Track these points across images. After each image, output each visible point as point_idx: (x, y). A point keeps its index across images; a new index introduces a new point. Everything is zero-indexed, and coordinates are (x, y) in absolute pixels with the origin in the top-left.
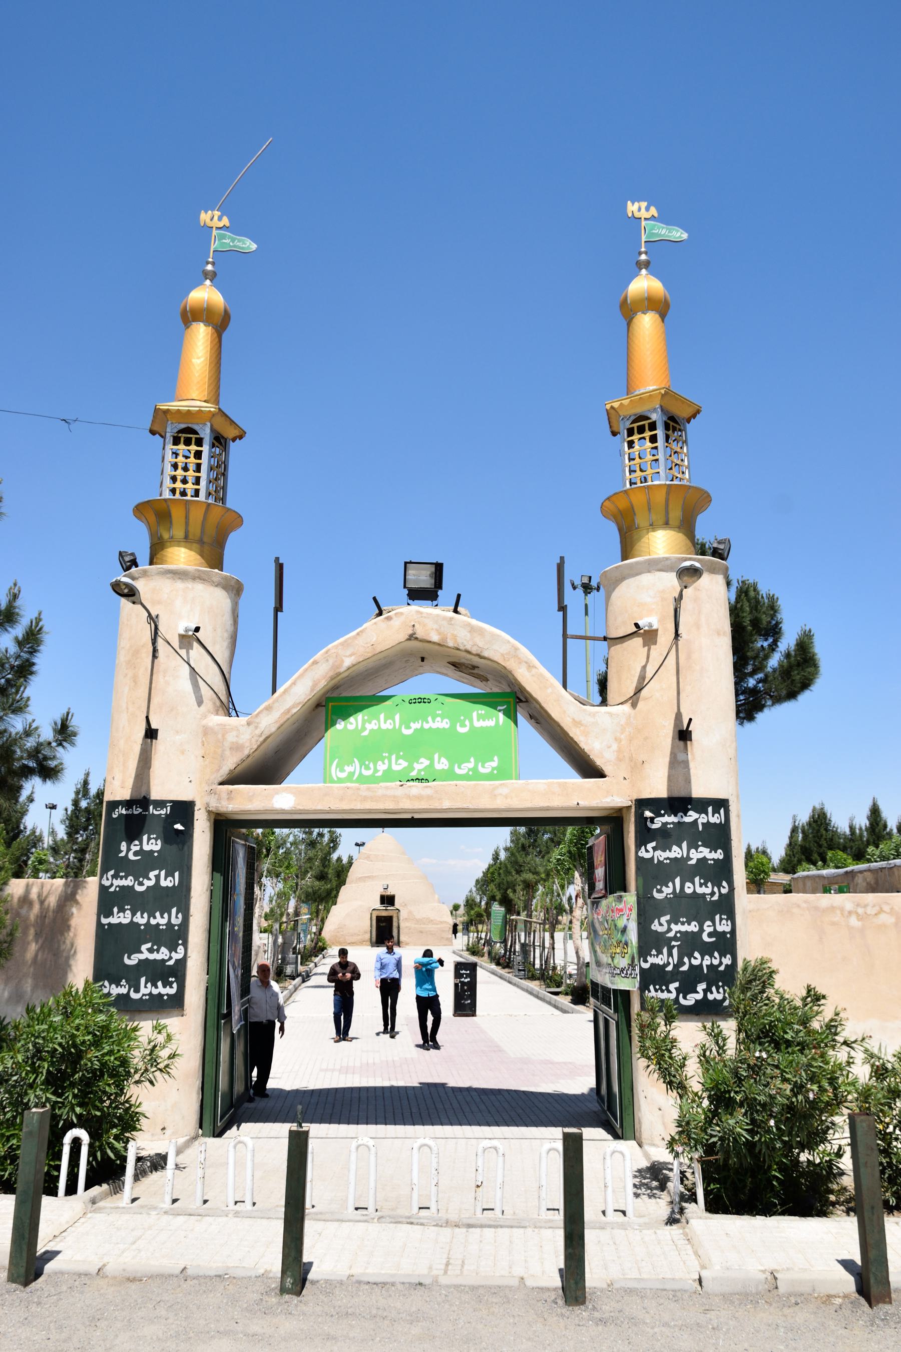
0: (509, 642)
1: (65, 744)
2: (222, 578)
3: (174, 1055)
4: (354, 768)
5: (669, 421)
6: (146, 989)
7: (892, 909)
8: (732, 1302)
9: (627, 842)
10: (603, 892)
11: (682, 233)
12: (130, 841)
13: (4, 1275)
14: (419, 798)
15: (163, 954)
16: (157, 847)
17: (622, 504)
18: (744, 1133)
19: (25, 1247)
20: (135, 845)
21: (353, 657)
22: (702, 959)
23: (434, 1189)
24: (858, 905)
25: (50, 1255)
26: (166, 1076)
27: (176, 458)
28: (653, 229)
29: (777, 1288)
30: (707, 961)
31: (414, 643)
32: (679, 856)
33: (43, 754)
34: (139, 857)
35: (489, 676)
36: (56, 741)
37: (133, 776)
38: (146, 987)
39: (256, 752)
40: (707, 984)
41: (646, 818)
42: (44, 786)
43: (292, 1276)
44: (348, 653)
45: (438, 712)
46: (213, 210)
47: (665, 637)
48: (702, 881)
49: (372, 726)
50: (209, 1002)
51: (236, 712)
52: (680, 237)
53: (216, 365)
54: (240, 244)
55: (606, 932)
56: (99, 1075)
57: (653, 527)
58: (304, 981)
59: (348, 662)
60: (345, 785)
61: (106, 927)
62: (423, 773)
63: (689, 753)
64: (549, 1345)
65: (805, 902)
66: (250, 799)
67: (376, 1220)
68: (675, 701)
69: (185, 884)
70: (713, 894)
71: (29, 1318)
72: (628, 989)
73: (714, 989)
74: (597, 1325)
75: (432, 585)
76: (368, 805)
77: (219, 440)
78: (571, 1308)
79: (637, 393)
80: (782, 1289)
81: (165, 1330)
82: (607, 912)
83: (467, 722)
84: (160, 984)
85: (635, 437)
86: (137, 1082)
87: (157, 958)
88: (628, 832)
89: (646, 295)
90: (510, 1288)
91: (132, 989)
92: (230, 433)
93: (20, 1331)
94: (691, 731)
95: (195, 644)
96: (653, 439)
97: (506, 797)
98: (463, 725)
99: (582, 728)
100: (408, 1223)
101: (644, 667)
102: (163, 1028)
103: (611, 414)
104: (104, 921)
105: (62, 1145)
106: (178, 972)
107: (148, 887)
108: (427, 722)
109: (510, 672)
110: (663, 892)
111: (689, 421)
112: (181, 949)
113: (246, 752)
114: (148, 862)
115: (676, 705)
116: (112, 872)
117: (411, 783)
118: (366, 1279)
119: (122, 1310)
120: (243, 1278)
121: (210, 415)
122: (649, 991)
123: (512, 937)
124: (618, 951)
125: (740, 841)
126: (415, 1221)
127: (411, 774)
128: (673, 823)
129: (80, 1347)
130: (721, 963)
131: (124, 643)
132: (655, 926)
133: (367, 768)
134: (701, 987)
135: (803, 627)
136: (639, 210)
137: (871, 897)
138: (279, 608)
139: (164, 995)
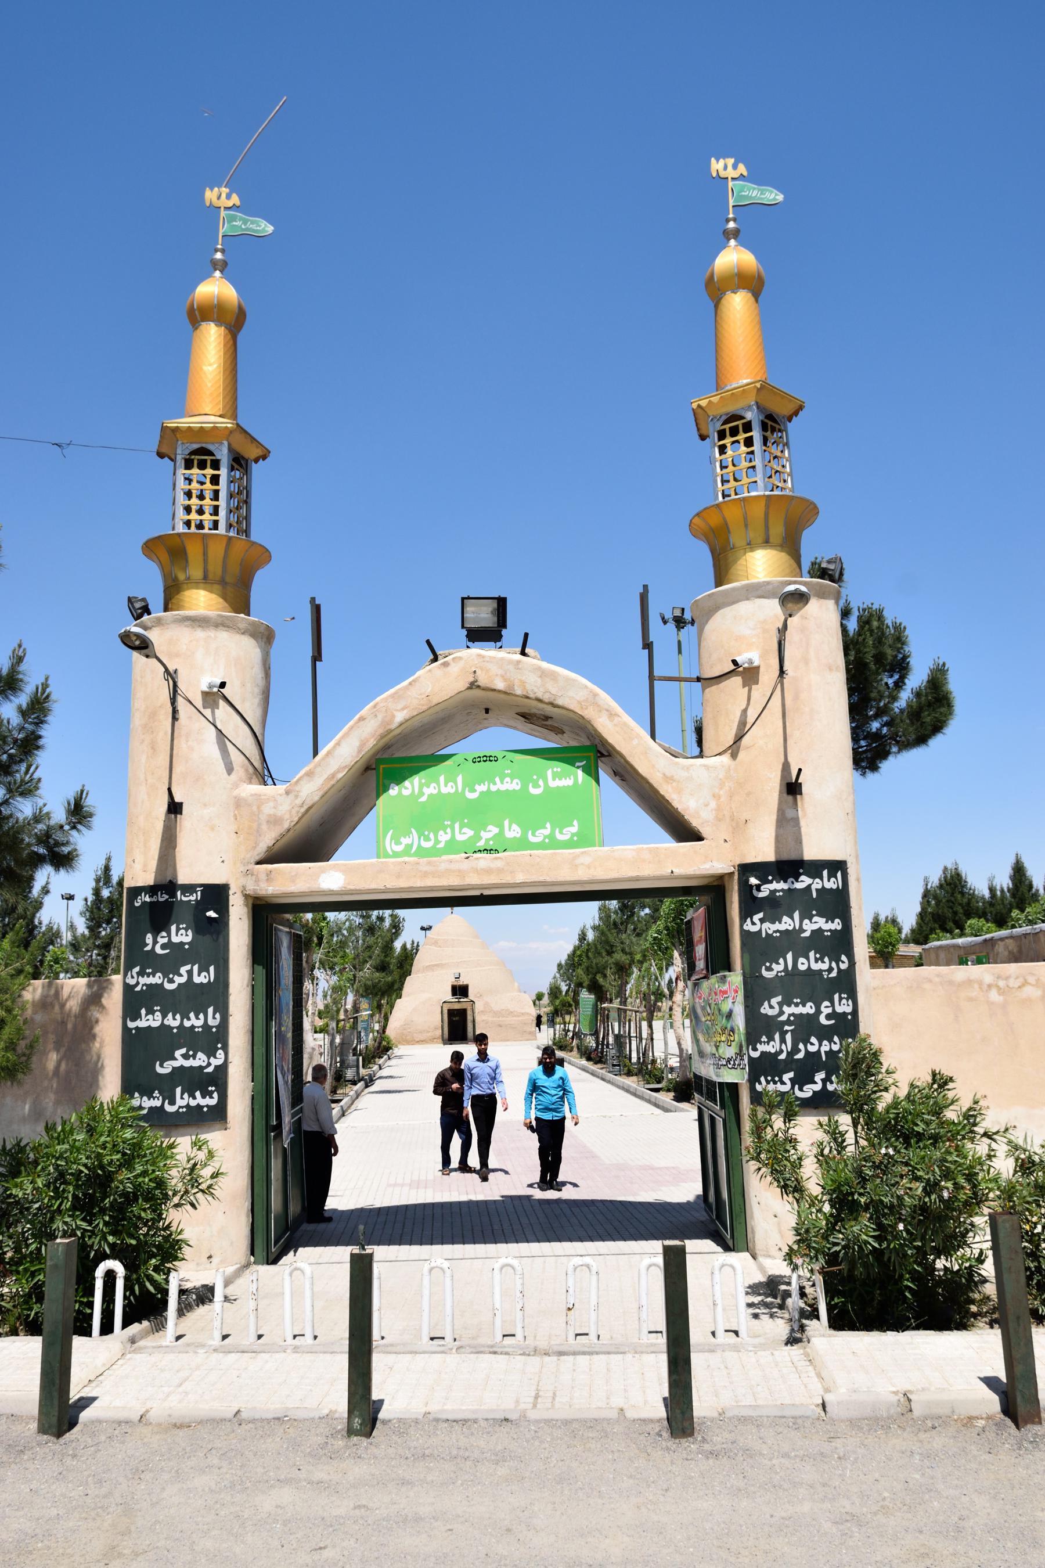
0: (586, 687)
2: (249, 624)
3: (217, 1174)
4: (412, 839)
5: (766, 421)
6: (182, 1100)
7: (1038, 980)
8: (860, 1428)
9: (731, 915)
10: (704, 972)
11: (776, 195)
12: (156, 933)
13: (34, 1426)
14: (488, 871)
15: (200, 1060)
16: (188, 939)
17: (714, 520)
18: (870, 1240)
19: (56, 1394)
20: (162, 937)
21: (405, 711)
22: (820, 1045)
23: (519, 1314)
24: (999, 977)
25: (85, 1402)
26: (210, 1198)
27: (190, 484)
28: (741, 192)
29: (911, 1411)
30: (825, 1047)
32: (791, 928)
34: (168, 951)
35: (565, 728)
37: (156, 857)
38: (182, 1098)
39: (298, 825)
40: (826, 1074)
41: (751, 886)
43: (360, 1416)
44: (400, 707)
45: (506, 772)
46: (219, 187)
47: (768, 675)
48: (818, 956)
49: (430, 790)
50: (256, 1112)
51: (272, 779)
52: (774, 199)
56: (130, 1199)
57: (751, 546)
58: (367, 1086)
59: (400, 717)
61: (134, 1032)
62: (491, 843)
63: (799, 809)
64: (653, 1482)
65: (938, 976)
66: (293, 879)
67: (454, 1351)
68: (782, 749)
69: (221, 979)
70: (830, 970)
71: (64, 1473)
72: (736, 1081)
73: (834, 1078)
74: (708, 1458)
75: (494, 623)
76: (430, 882)
77: (239, 462)
78: (677, 1441)
79: (728, 388)
80: (917, 1412)
81: (219, 1480)
82: (710, 995)
83: (541, 782)
84: (198, 1094)
85: (728, 441)
86: (177, 1206)
88: (732, 902)
89: (736, 271)
90: (608, 1420)
91: (167, 1101)
92: (251, 452)
93: (54, 1487)
94: (801, 784)
95: (222, 703)
96: (749, 442)
97: (589, 867)
98: (538, 786)
99: (674, 784)
100: (490, 1353)
101: (745, 711)
102: (204, 1144)
103: (698, 414)
104: (131, 1025)
105: (94, 1279)
106: (218, 1080)
108: (495, 784)
109: (589, 722)
110: (773, 970)
111: (790, 419)
112: (220, 1054)
113: (286, 825)
114: (178, 956)
116: (137, 969)
117: (478, 855)
118: (444, 1416)
119: (169, 1459)
120: (305, 1420)
121: (227, 433)
122: (760, 1083)
123: (604, 1028)
124: (723, 1039)
125: (860, 908)
126: (499, 1350)
128: (782, 890)
129: (123, 1502)
131: (139, 704)
132: (765, 1009)
133: (427, 839)
134: (819, 1076)
136: (725, 168)
137: (1013, 968)
138: (317, 657)
139: (203, 1107)
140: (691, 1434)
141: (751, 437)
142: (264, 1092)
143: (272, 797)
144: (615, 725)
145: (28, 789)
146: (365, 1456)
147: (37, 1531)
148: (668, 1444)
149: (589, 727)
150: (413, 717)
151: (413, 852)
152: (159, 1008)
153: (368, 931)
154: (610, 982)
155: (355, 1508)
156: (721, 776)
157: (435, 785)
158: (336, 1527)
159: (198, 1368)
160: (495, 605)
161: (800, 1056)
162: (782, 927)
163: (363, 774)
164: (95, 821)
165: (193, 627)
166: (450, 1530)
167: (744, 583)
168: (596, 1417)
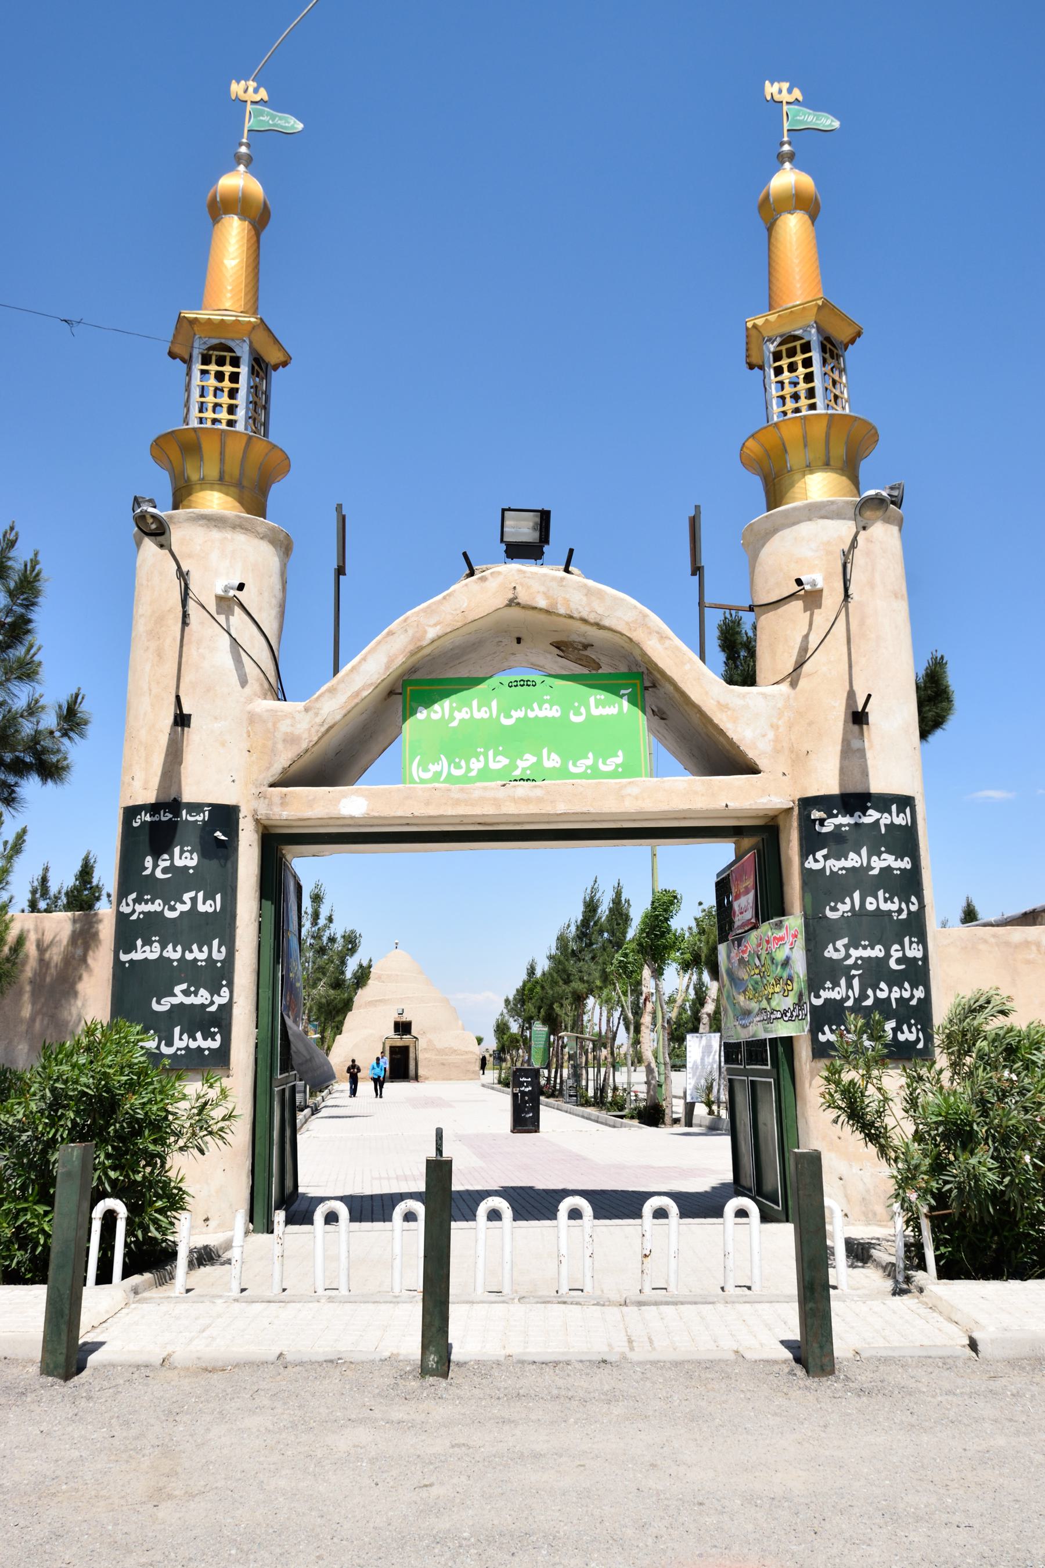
0: (635, 607)
1: (71, 734)
2: (269, 529)
3: (230, 1116)
5: (825, 342)
6: (181, 1042)
10: (753, 921)
11: (832, 121)
13: (34, 1369)
14: (527, 800)
15: (203, 997)
16: (193, 863)
19: (64, 1327)
20: (163, 860)
21: (438, 627)
22: (890, 991)
23: (588, 1261)
25: (94, 1347)
26: (220, 1143)
30: (896, 993)
31: (515, 612)
32: (858, 865)
33: (42, 746)
34: (170, 875)
36: (60, 730)
37: (159, 773)
38: (181, 1039)
39: (317, 747)
40: (897, 1022)
41: (815, 820)
42: (44, 787)
44: (432, 621)
45: (545, 697)
46: (247, 79)
47: (832, 599)
48: (887, 895)
49: (462, 715)
50: (259, 1062)
52: (830, 125)
53: (254, 269)
54: (282, 123)
55: (757, 971)
56: (137, 1127)
57: (809, 468)
58: (313, 1114)
59: (432, 633)
60: (432, 785)
61: (127, 965)
63: (866, 740)
67: (516, 1301)
68: (847, 677)
69: (229, 909)
70: (900, 911)
71: (81, 1414)
73: (905, 1027)
74: (859, 1396)
77: (260, 367)
78: (816, 1379)
79: (785, 306)
81: (275, 1420)
82: (759, 945)
83: (583, 710)
84: (199, 1035)
85: (784, 363)
86: (181, 1149)
87: (195, 1003)
88: (789, 841)
89: (794, 192)
90: (726, 1362)
91: (163, 1042)
92: (273, 356)
93: (70, 1429)
95: (237, 610)
97: (637, 798)
98: (578, 713)
99: (729, 713)
100: (559, 1303)
101: (806, 637)
103: (753, 336)
104: (124, 957)
107: (181, 912)
109: (638, 645)
110: (838, 910)
112: (225, 992)
113: (304, 745)
114: (181, 880)
115: (848, 680)
116: (134, 896)
118: (531, 1358)
119: (208, 1401)
120: (363, 1362)
121: (250, 328)
122: (824, 1033)
123: (557, 1061)
124: (777, 989)
126: (569, 1300)
127: (514, 774)
128: (848, 825)
129: (160, 1444)
130: (912, 996)
132: (830, 953)
133: (458, 766)
135: (934, 653)
136: (780, 91)
138: (340, 571)
139: (204, 1050)
140: (832, 1372)
141: (811, 358)
142: (269, 1040)
143: (290, 713)
144: (666, 649)
145: (27, 671)
146: (449, 1397)
147: (58, 1473)
148: (807, 1383)
149: (636, 653)
150: (446, 634)
151: (442, 780)
152: (157, 938)
153: (319, 952)
154: (565, 1012)
155: (453, 1447)
156: (780, 705)
157: (467, 709)
158: (437, 1464)
159: (219, 1316)
160: (538, 520)
161: (869, 1002)
162: (849, 864)
163: (385, 699)
164: (90, 730)
165: (208, 527)
166: (581, 1466)
167: (806, 502)
168: (710, 1358)
